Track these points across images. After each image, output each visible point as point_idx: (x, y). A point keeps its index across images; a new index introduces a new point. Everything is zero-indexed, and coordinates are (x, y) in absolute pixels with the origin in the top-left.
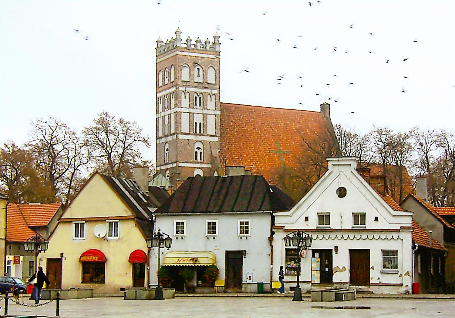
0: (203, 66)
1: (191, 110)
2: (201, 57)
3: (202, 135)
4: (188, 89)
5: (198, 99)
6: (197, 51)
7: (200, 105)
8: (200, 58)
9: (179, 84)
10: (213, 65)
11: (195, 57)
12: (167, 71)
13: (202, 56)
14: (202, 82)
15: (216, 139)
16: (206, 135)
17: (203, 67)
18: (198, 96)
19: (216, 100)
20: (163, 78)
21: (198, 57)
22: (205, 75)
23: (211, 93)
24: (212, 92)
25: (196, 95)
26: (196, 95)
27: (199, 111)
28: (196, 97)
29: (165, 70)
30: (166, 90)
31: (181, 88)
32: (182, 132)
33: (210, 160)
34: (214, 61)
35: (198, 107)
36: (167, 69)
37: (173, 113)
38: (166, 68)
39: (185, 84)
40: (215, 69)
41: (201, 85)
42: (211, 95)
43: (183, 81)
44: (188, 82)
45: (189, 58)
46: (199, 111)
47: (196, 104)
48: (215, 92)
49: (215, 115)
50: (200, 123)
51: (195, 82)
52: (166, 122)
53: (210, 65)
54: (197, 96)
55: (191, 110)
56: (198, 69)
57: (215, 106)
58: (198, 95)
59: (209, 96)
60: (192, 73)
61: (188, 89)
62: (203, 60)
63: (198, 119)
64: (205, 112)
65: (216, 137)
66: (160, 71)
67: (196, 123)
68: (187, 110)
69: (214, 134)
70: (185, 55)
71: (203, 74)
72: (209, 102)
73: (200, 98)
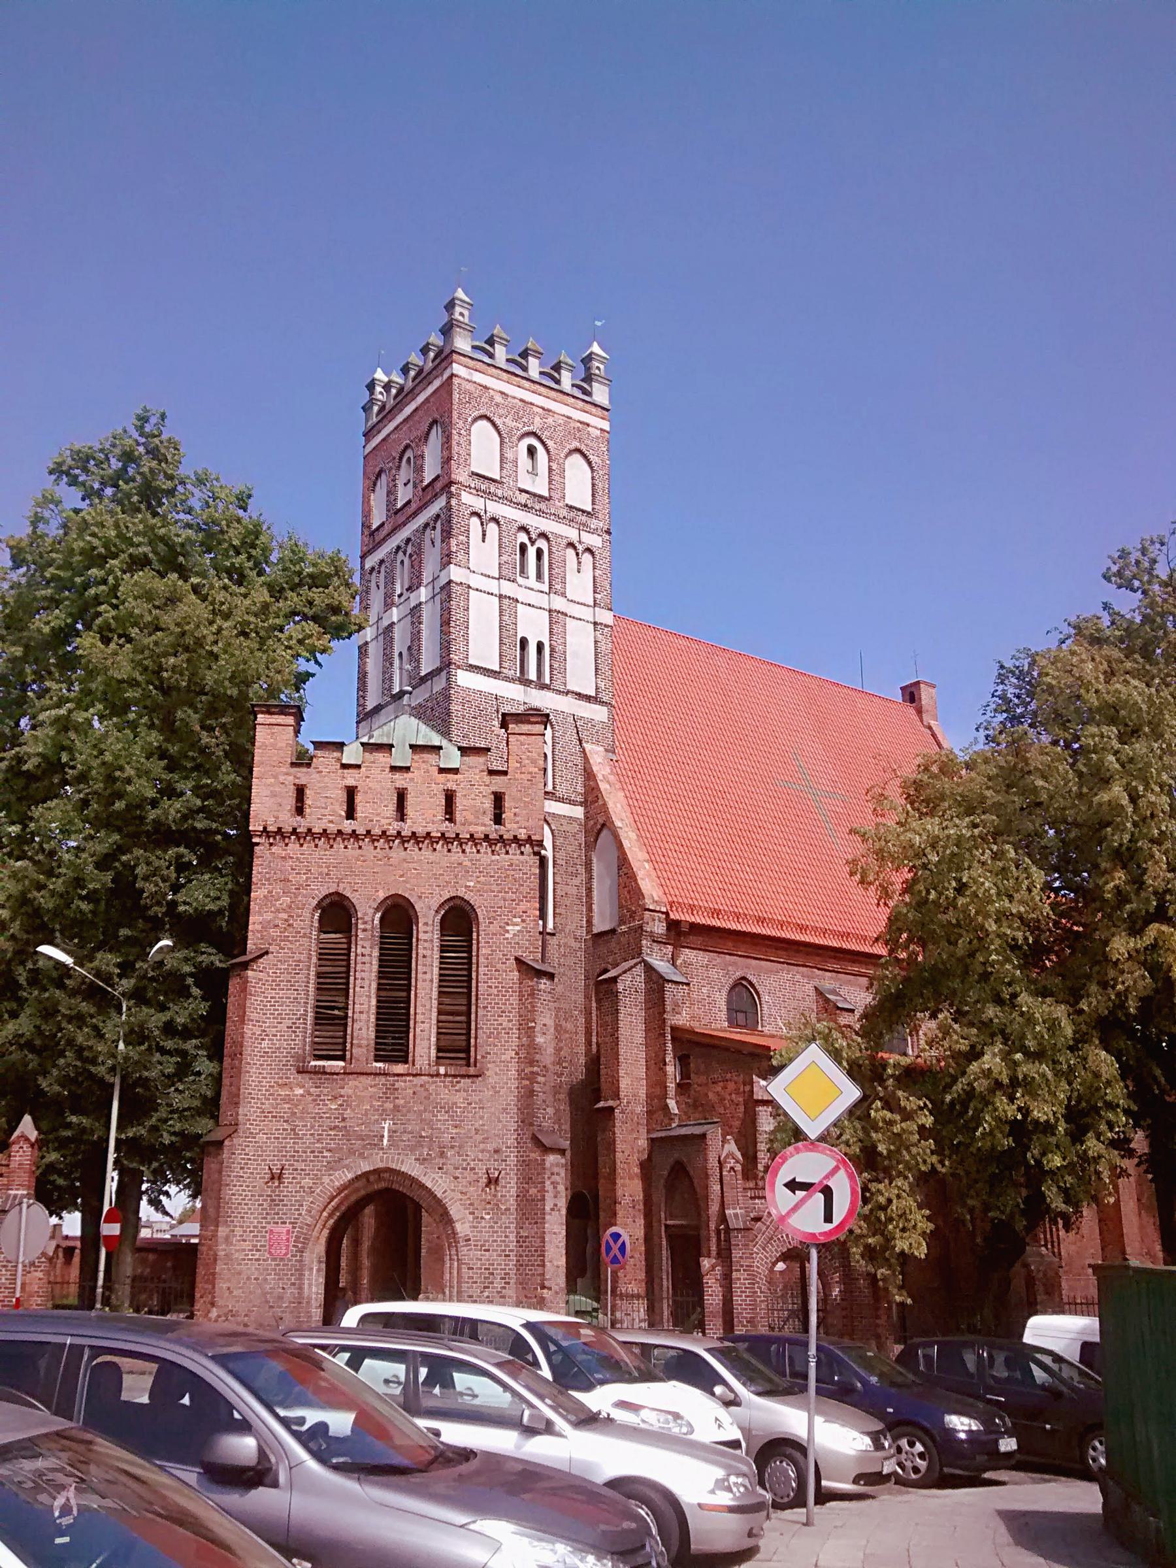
0: (551, 438)
1: (508, 588)
2: (543, 409)
3: (543, 687)
4: (495, 508)
5: (532, 552)
6: (527, 384)
7: (539, 576)
8: (540, 411)
9: (461, 479)
10: (583, 448)
11: (521, 400)
12: (409, 460)
13: (546, 407)
14: (546, 494)
15: (599, 713)
16: (562, 688)
17: (550, 443)
18: (533, 543)
19: (598, 572)
20: (391, 492)
21: (532, 404)
22: (555, 475)
23: (580, 542)
24: (583, 540)
25: (523, 538)
26: (523, 538)
27: (534, 598)
28: (523, 548)
29: (401, 458)
30: (404, 524)
31: (466, 498)
32: (471, 661)
33: (580, 789)
34: (589, 434)
35: (532, 581)
36: (409, 453)
37: (433, 597)
38: (407, 447)
39: (483, 487)
40: (589, 463)
41: (543, 506)
42: (580, 548)
43: (473, 473)
44: (494, 481)
45: (498, 399)
46: (534, 598)
47: (523, 571)
48: (594, 541)
49: (595, 624)
50: (540, 646)
51: (522, 491)
52: (400, 643)
53: (575, 444)
54: (529, 544)
55: (508, 588)
56: (531, 451)
57: (595, 592)
58: (530, 539)
59: (570, 552)
60: (509, 455)
61: (495, 508)
62: (550, 420)
63: (533, 626)
64: (558, 603)
65: (597, 707)
66: (379, 475)
67: (524, 642)
68: (493, 586)
69: (593, 694)
70: (484, 384)
71: (550, 469)
72: (572, 577)
73: (539, 553)
